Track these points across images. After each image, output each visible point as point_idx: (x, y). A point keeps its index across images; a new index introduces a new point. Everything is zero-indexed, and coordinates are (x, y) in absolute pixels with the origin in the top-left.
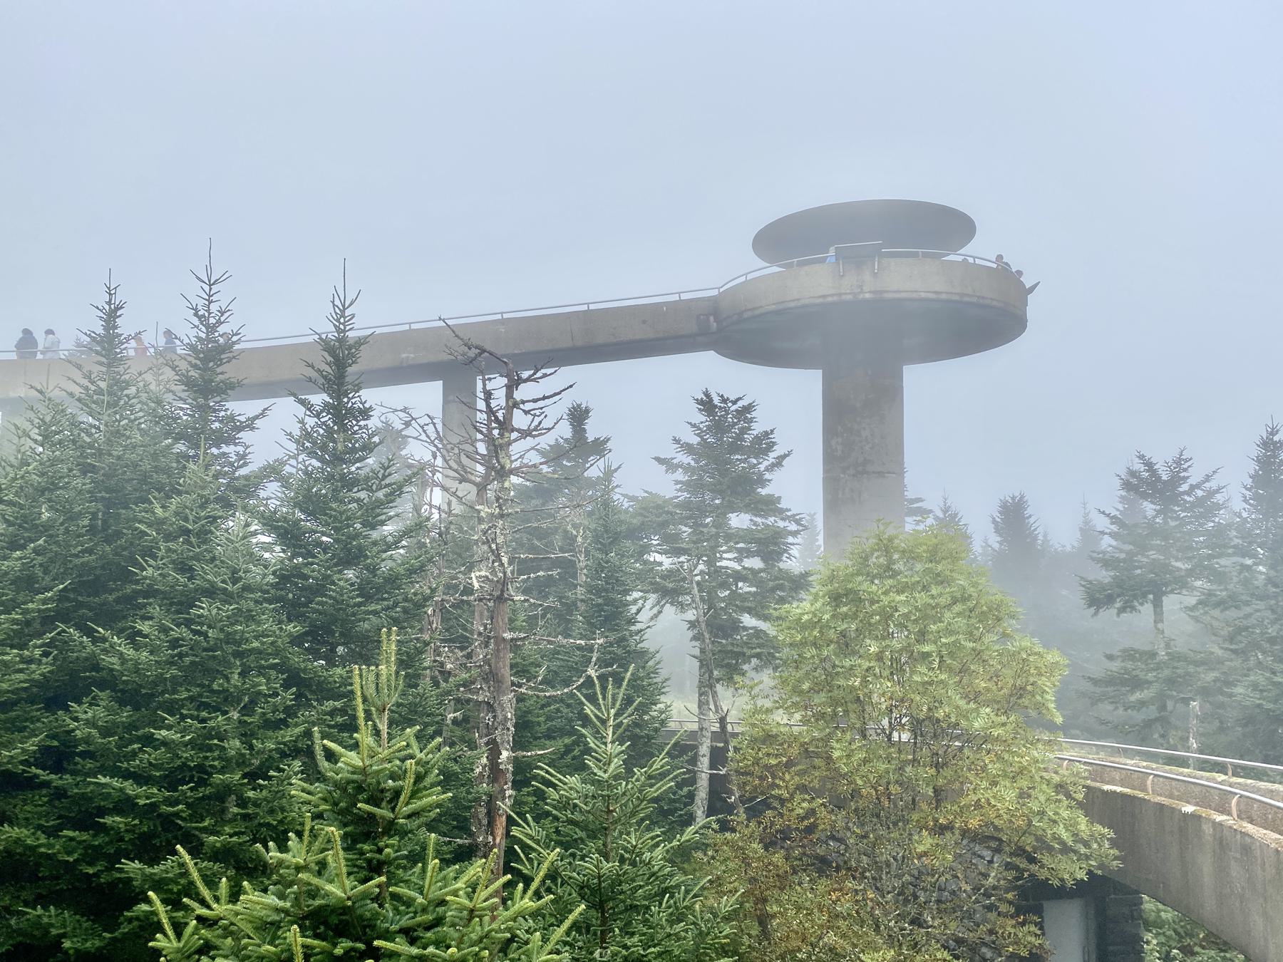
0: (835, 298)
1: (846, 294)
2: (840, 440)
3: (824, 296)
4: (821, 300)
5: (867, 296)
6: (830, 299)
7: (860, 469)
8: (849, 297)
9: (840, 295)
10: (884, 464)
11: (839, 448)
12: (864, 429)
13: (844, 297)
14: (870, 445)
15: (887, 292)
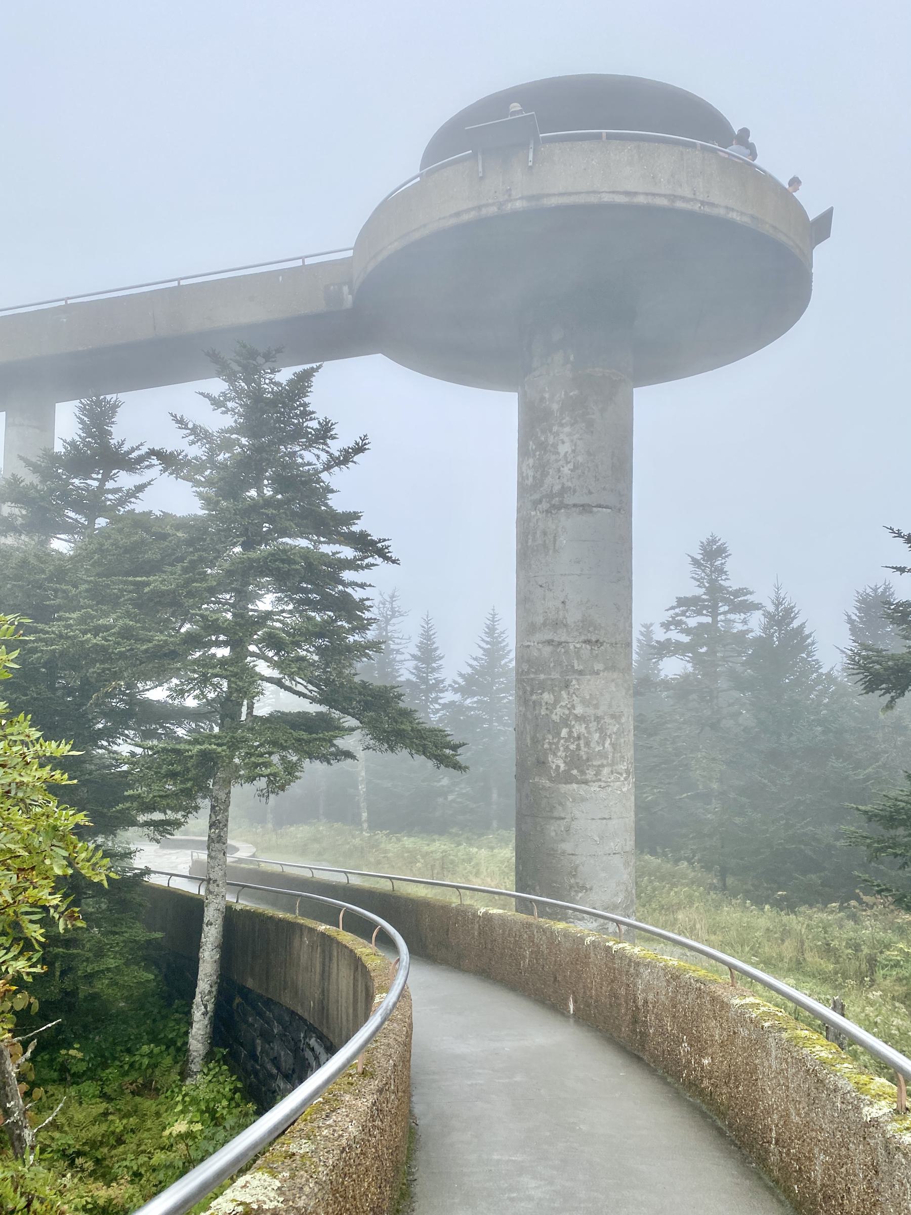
0: (472, 215)
1: (487, 205)
2: (531, 461)
3: (458, 214)
4: (453, 221)
5: (519, 205)
6: (465, 218)
7: (556, 501)
8: (493, 210)
9: (479, 208)
10: (590, 493)
11: (531, 473)
12: (563, 442)
13: (484, 211)
14: (571, 466)
15: (554, 195)
